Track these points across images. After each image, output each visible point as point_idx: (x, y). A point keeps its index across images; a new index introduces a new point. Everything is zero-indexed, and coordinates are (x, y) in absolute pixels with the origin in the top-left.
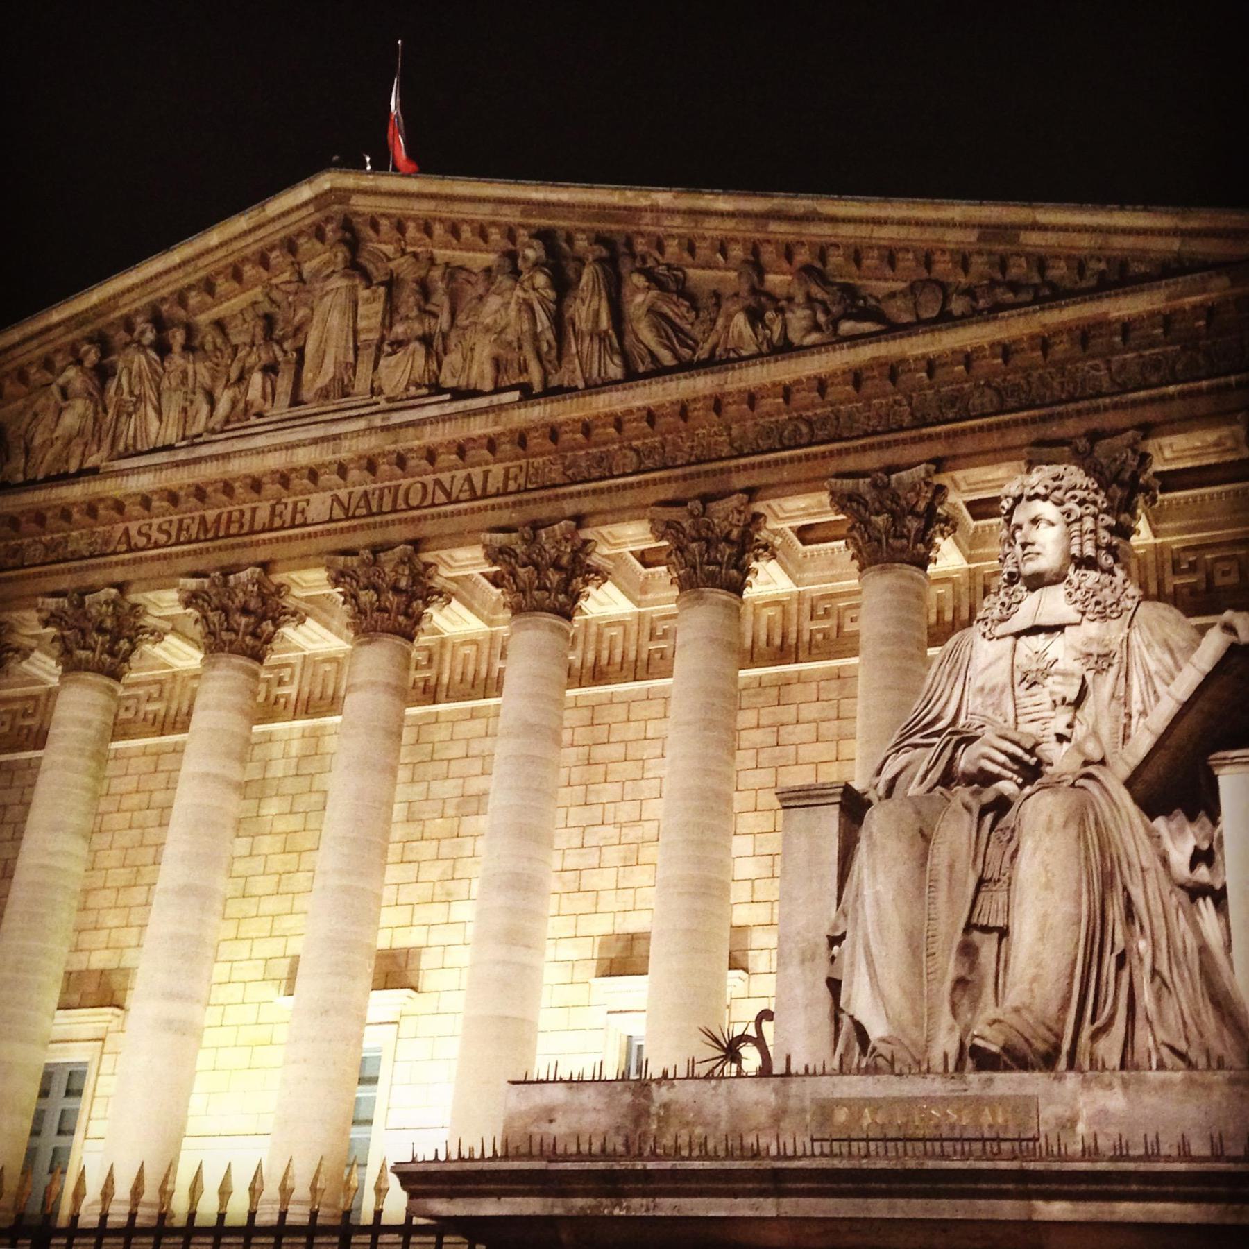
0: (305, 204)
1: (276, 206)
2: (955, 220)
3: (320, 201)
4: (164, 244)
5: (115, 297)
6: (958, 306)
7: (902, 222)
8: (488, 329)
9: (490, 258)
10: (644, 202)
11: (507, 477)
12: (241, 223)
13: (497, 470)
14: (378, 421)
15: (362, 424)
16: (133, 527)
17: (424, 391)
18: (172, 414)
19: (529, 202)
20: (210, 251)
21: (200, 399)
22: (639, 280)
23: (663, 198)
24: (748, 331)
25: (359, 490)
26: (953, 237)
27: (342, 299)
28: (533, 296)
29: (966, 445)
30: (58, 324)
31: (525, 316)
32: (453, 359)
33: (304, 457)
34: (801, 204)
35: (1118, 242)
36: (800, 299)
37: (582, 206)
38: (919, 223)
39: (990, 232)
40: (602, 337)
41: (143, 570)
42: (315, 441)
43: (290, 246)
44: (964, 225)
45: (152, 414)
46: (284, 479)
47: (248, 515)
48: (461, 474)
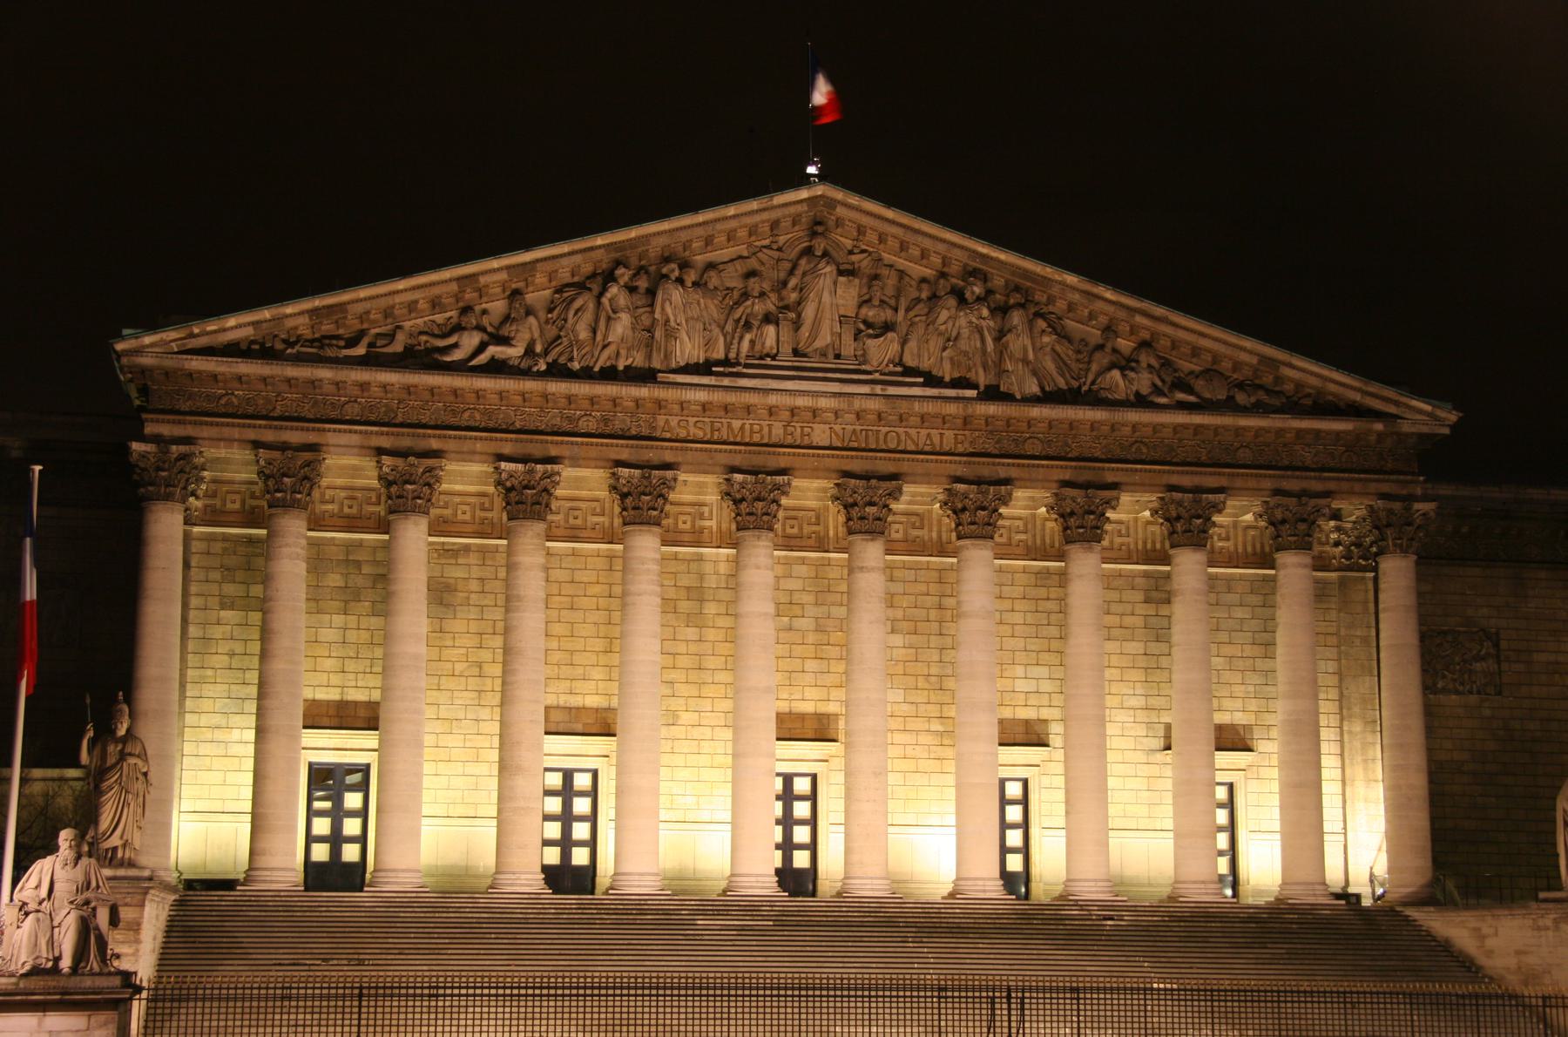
0: (801, 201)
1: (780, 199)
2: (1246, 350)
3: (812, 201)
4: (695, 208)
5: (647, 237)
6: (1241, 398)
7: (1216, 340)
8: (940, 334)
9: (928, 272)
10: (1057, 277)
11: (956, 443)
12: (754, 205)
13: (949, 434)
14: (878, 389)
15: (865, 389)
16: (674, 421)
17: (899, 369)
18: (699, 340)
19: (974, 252)
20: (726, 218)
21: (716, 331)
22: (1041, 324)
23: (1071, 279)
24: (1121, 382)
25: (849, 428)
26: (1244, 357)
27: (829, 281)
28: (984, 323)
29: (1239, 483)
30: (600, 247)
31: (977, 336)
32: (912, 345)
33: (823, 403)
34: (1159, 311)
35: (1332, 387)
36: (1144, 365)
37: (1012, 265)
38: (1225, 343)
39: (1264, 359)
40: (1025, 361)
41: (689, 456)
42: (835, 395)
43: (775, 225)
44: (1250, 352)
45: (686, 338)
46: (793, 411)
47: (766, 430)
48: (924, 432)
